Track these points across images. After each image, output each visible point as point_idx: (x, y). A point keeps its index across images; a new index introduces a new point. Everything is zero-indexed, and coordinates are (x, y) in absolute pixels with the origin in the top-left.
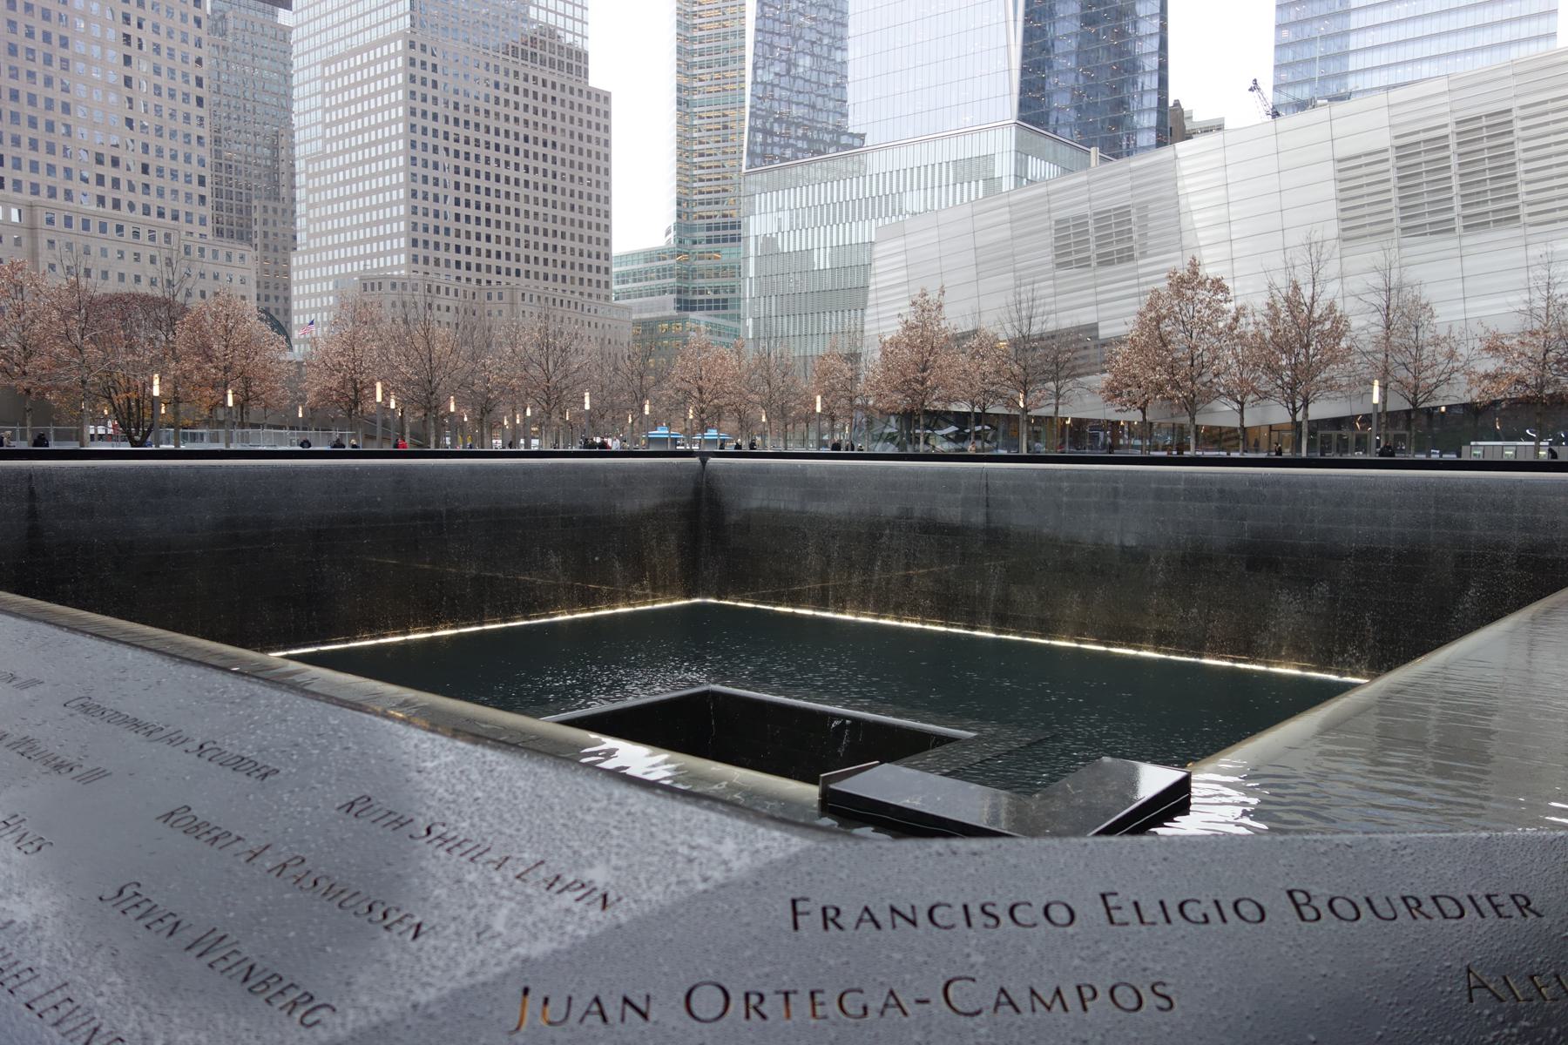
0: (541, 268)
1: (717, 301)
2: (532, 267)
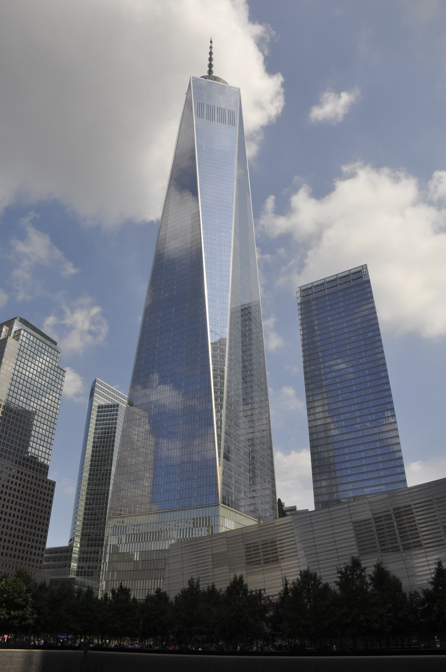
0: (13, 553)
1: (88, 572)
2: (9, 552)
